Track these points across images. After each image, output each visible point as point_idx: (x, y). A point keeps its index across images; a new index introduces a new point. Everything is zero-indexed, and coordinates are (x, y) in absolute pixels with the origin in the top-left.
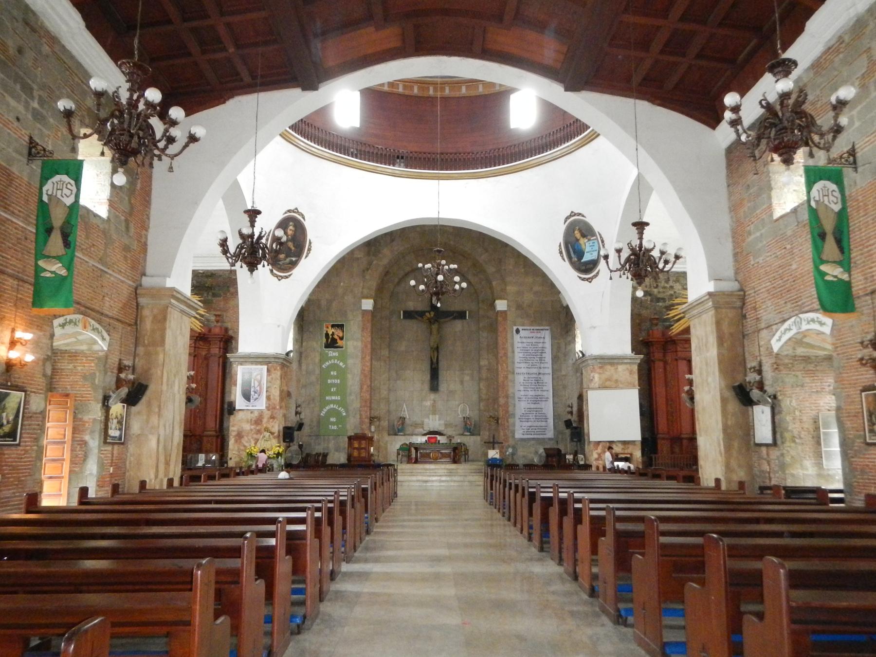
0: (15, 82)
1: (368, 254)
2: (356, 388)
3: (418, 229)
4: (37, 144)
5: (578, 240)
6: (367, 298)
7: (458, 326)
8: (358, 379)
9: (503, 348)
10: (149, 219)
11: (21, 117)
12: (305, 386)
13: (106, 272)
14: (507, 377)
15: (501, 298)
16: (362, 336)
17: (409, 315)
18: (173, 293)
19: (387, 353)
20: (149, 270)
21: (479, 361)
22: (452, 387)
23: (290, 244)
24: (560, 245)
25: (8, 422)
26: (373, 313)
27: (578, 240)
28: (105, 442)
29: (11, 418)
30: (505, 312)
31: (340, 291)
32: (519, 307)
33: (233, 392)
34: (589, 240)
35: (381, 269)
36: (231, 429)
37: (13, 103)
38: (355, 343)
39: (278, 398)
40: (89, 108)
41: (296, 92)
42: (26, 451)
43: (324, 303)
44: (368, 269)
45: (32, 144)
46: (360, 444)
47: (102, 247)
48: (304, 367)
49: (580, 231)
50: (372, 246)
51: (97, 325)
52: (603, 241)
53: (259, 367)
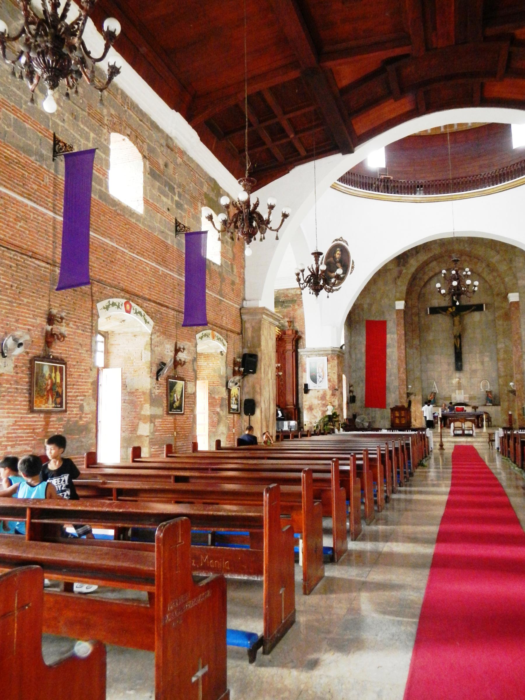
0: (165, 186)
1: (398, 265)
2: (395, 371)
3: (438, 242)
4: (180, 224)
6: (399, 300)
7: (476, 316)
8: (395, 363)
9: (517, 333)
10: (244, 261)
11: (170, 208)
12: (354, 371)
13: (223, 301)
15: (512, 292)
16: (397, 330)
17: (434, 311)
18: (264, 311)
20: (247, 297)
21: (496, 344)
22: (474, 367)
25: (177, 400)
26: (405, 311)
28: (229, 413)
29: (179, 397)
30: (517, 303)
31: (378, 296)
33: (304, 377)
35: (409, 276)
36: (304, 403)
37: (164, 199)
38: (392, 336)
40: (206, 193)
41: (338, 157)
42: (188, 418)
43: (366, 306)
44: (399, 277)
46: (400, 414)
47: (219, 284)
48: (353, 356)
50: (402, 259)
51: (220, 336)
53: (322, 358)
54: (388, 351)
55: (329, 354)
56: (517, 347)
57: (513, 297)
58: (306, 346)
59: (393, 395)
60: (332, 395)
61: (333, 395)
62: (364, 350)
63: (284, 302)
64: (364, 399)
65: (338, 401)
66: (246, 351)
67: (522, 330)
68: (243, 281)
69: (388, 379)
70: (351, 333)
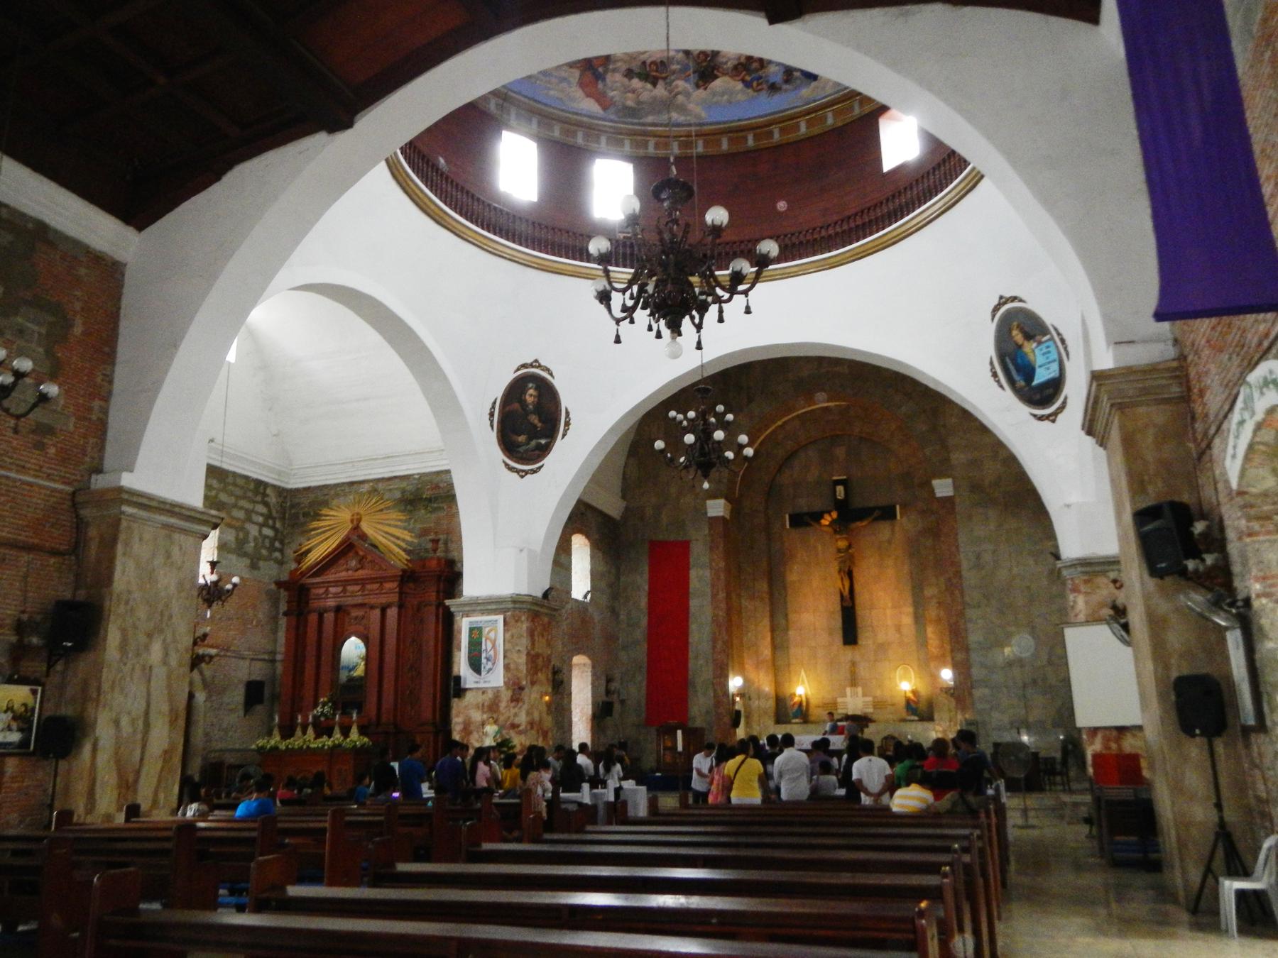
5: (1020, 347)
10: (111, 382)
12: (625, 648)
14: (961, 614)
16: (712, 560)
17: (799, 521)
19: (765, 586)
22: (881, 638)
23: (534, 419)
24: (991, 363)
27: (1020, 347)
31: (673, 490)
32: (976, 487)
33: (456, 659)
34: (1040, 343)
39: (523, 668)
41: (321, 137)
43: (649, 512)
52: (1063, 341)
54: (694, 603)
55: (508, 610)
56: (952, 594)
57: (943, 487)
58: (465, 593)
59: (702, 700)
60: (512, 700)
61: (515, 700)
62: (644, 602)
63: (430, 500)
64: (644, 709)
65: (528, 714)
66: (82, 595)
67: (962, 556)
69: (691, 664)
70: (618, 569)
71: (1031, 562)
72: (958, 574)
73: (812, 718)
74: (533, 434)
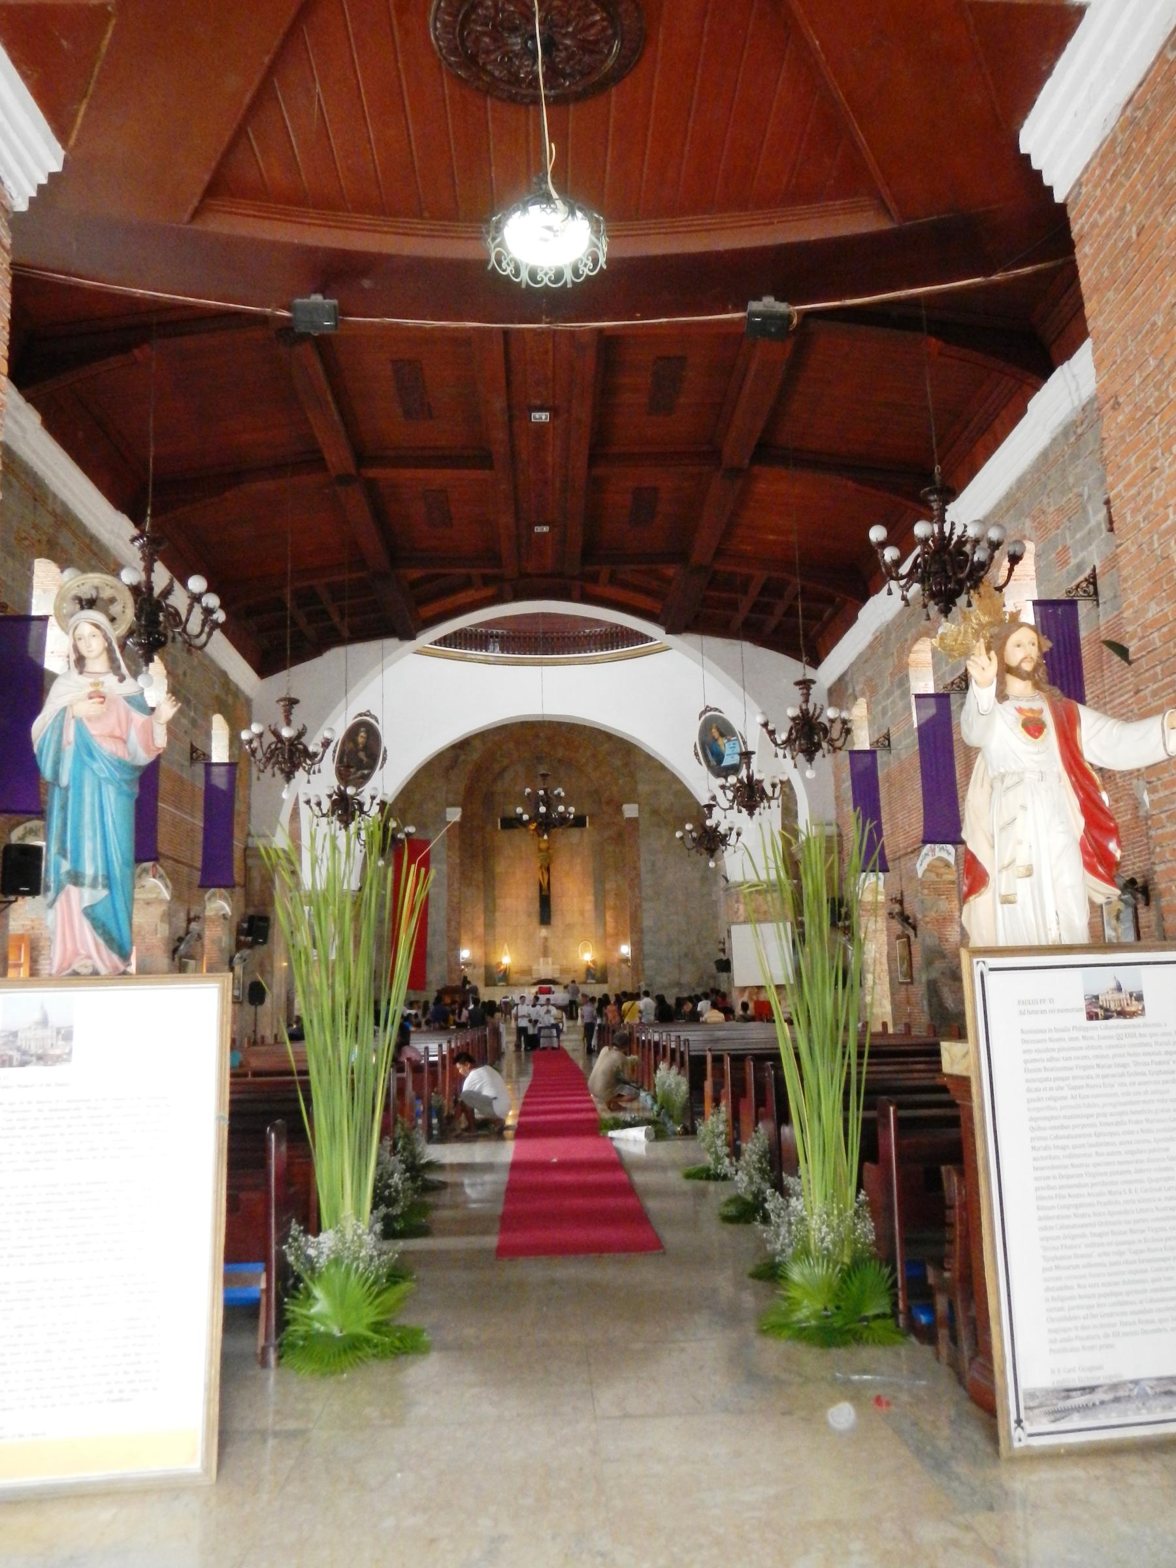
6: (453, 805)
8: (443, 914)
15: (628, 802)
16: (448, 857)
17: (511, 823)
20: (253, 832)
23: (362, 755)
26: (461, 825)
27: (716, 740)
30: (635, 820)
32: (655, 812)
35: (470, 767)
38: (439, 866)
44: (452, 767)
45: (193, 750)
49: (718, 730)
50: (463, 746)
57: (630, 810)
66: (251, 911)
67: (642, 863)
68: (249, 808)
71: (689, 869)
72: (638, 875)
73: (511, 981)
74: (360, 765)
